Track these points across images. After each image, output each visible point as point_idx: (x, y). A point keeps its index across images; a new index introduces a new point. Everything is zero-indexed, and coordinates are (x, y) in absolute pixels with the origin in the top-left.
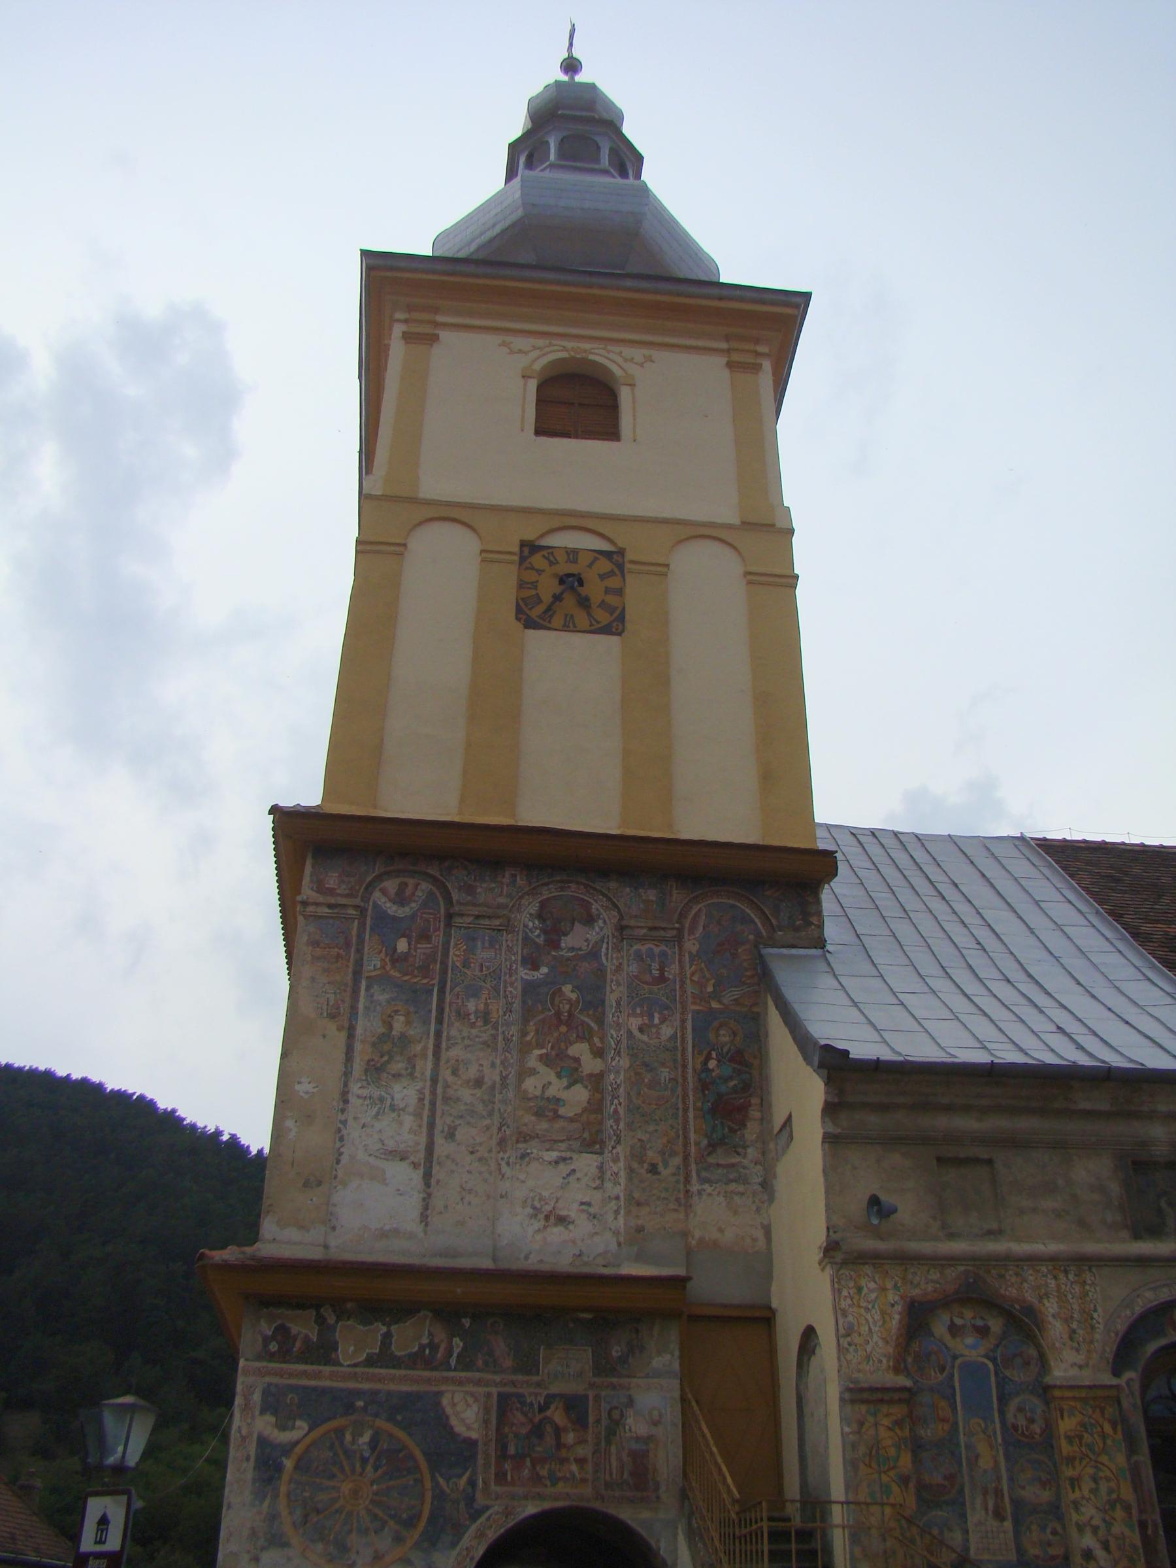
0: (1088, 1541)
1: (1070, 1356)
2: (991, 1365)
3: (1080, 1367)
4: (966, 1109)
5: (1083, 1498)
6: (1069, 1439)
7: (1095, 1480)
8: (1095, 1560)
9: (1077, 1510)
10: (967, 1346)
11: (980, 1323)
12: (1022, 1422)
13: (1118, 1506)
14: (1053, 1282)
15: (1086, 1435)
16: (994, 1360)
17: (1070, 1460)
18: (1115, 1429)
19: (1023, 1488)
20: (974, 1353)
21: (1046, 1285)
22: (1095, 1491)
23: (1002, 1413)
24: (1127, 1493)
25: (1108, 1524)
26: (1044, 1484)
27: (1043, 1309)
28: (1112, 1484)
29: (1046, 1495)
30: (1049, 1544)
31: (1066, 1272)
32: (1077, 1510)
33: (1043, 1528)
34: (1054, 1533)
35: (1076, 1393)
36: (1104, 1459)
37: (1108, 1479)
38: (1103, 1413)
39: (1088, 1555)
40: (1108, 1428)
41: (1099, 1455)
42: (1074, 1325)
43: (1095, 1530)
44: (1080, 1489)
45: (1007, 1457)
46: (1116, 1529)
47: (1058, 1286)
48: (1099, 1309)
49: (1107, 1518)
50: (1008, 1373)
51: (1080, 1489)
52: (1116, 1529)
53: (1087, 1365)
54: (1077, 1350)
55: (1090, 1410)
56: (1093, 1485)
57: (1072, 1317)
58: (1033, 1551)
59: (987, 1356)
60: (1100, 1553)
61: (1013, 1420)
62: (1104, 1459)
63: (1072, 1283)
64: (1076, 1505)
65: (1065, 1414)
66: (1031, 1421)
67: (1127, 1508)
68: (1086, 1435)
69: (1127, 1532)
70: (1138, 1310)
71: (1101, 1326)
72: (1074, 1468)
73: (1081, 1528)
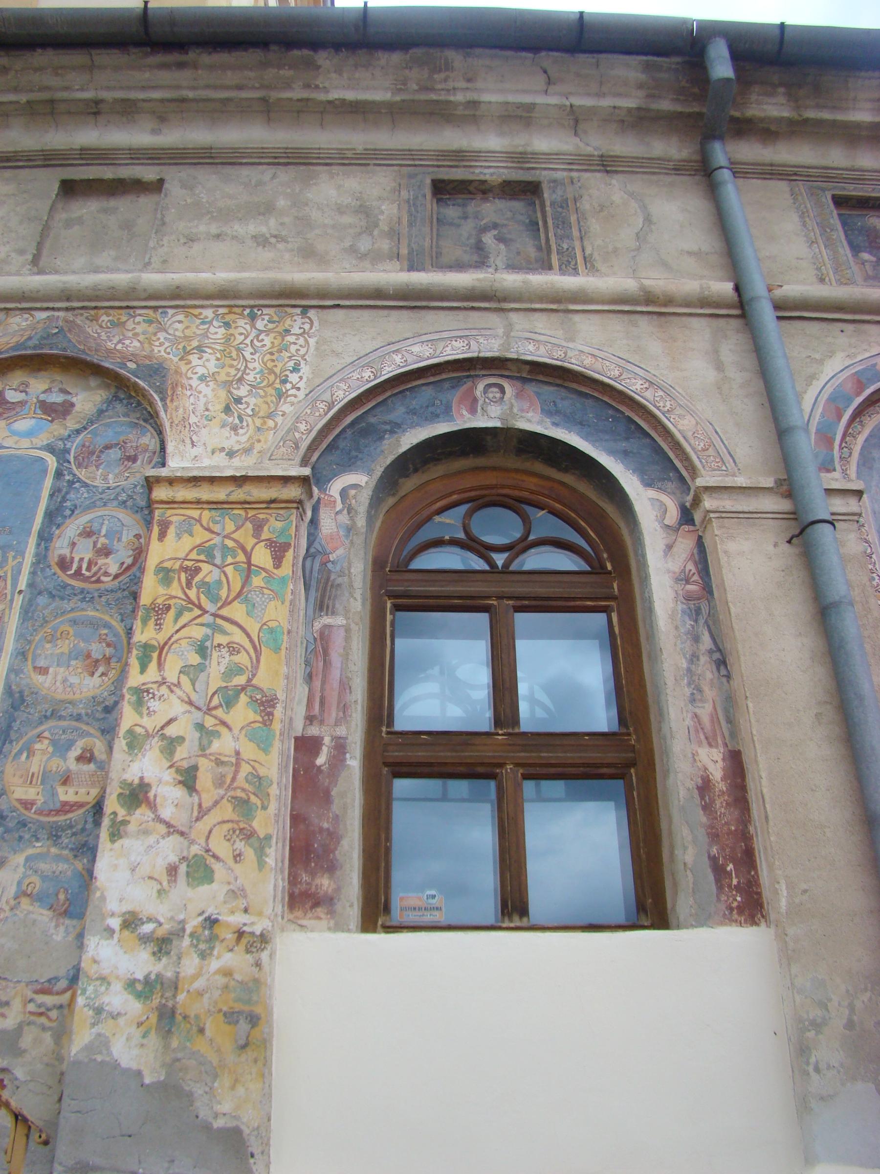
0: (149, 766)
1: (216, 435)
2: (52, 462)
3: (231, 454)
4: (127, 110)
5: (163, 682)
6: (165, 575)
7: (202, 650)
8: (152, 806)
9: (139, 704)
10: (14, 433)
11: (56, 398)
12: (84, 552)
13: (243, 698)
14: (222, 331)
15: (206, 568)
16: (61, 454)
17: (159, 611)
18: (278, 560)
19: (44, 671)
20: (25, 443)
21: (205, 335)
22: (192, 672)
23: (45, 538)
24: (276, 674)
25: (205, 734)
26: (92, 665)
27: (184, 368)
28: (242, 659)
29: (90, 686)
30: (66, 780)
31: (253, 318)
32: (139, 704)
33: (61, 748)
34: (86, 757)
35: (205, 493)
36: (237, 611)
37: (233, 649)
38: (258, 528)
39: (138, 795)
40: (262, 557)
41: (227, 603)
42: (243, 391)
43: (171, 745)
44: (160, 665)
45: (27, 612)
46: (224, 744)
47: (228, 338)
48: (305, 369)
49: (209, 722)
50: (82, 474)
51: (160, 665)
52: (224, 744)
53: (247, 451)
54: (235, 429)
55: (230, 526)
56: (195, 659)
57: (241, 380)
58: (21, 792)
59: (50, 449)
60: (169, 795)
61: (66, 552)
62: (237, 611)
63: (261, 332)
64: (141, 694)
65: (172, 532)
66: (106, 552)
67: (266, 705)
68: (206, 568)
69: (249, 751)
70: (388, 372)
71: (301, 395)
72: (159, 625)
73: (135, 743)
